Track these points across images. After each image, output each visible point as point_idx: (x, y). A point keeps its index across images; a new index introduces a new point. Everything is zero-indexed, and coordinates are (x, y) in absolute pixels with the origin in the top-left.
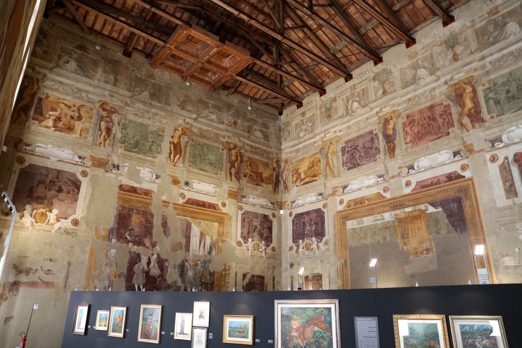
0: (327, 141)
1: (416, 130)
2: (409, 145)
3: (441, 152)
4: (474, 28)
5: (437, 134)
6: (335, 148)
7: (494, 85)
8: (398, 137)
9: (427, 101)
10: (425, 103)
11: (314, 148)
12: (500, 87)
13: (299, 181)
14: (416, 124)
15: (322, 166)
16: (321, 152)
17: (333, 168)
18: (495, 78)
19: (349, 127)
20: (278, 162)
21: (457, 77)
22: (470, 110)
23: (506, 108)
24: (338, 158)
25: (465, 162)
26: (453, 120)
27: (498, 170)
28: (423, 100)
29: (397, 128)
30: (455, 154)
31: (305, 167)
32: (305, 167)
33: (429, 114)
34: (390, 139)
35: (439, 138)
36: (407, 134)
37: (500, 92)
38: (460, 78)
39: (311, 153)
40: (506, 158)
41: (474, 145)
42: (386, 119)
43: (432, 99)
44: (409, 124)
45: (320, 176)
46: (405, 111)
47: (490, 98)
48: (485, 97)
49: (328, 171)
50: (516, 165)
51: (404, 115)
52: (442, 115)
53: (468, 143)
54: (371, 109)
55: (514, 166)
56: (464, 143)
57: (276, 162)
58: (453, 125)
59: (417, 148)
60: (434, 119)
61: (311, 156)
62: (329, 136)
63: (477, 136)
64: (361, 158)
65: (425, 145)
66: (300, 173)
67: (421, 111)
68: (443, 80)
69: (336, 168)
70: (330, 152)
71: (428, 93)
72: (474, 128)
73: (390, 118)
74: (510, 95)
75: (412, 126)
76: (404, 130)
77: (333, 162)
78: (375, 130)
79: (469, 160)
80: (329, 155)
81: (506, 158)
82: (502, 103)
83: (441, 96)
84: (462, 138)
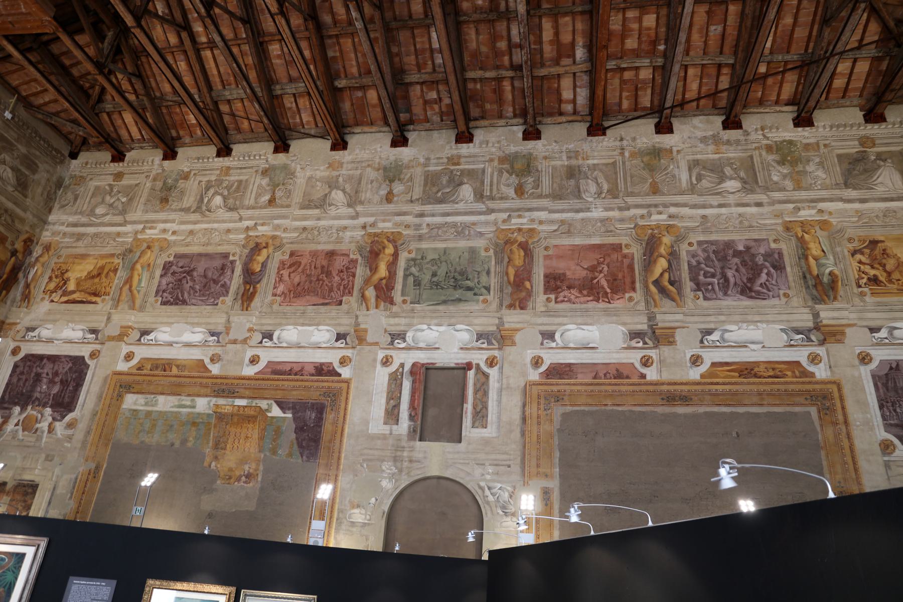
0: (144, 240)
1: (297, 280)
2: (278, 298)
3: (321, 327)
4: (427, 169)
5: (324, 298)
6: (152, 258)
7: (422, 258)
8: (265, 281)
9: (329, 243)
10: (325, 243)
11: (115, 244)
12: (428, 263)
13: (60, 292)
14: (300, 270)
15: (116, 281)
16: (124, 255)
17: (135, 292)
18: (427, 249)
19: (191, 232)
20: (29, 243)
21: (381, 225)
22: (381, 280)
23: (424, 297)
24: (152, 277)
25: (348, 353)
26: (353, 285)
27: (387, 378)
28: (323, 238)
29: (269, 264)
30: (340, 337)
31: (82, 271)
32: (82, 271)
33: (325, 263)
34: (251, 278)
35: (326, 304)
36: (281, 280)
37: (425, 271)
38: (384, 228)
39: (105, 251)
40: (402, 365)
41: (369, 332)
42: (257, 244)
43: (338, 243)
44: (290, 267)
45: (107, 297)
46: (291, 243)
47: (411, 274)
48: (406, 270)
49: (124, 294)
50: (411, 379)
51: (288, 248)
52: (342, 271)
53: (362, 326)
54: (241, 219)
55: (407, 379)
56: (357, 324)
57: (25, 241)
58: (350, 293)
59: (288, 308)
60: (329, 274)
61: (103, 257)
62: (151, 234)
63: (376, 321)
64: (192, 292)
65: (302, 308)
66: (68, 279)
67: (314, 254)
68: (362, 220)
69: (142, 293)
70: (141, 261)
71: (334, 231)
72: (377, 307)
73: (264, 245)
74: (435, 279)
75: (293, 272)
76: (278, 273)
77: (140, 281)
78: (233, 255)
79: (355, 352)
80: (138, 266)
81: (402, 365)
82: (422, 287)
83: (350, 242)
84: (357, 317)
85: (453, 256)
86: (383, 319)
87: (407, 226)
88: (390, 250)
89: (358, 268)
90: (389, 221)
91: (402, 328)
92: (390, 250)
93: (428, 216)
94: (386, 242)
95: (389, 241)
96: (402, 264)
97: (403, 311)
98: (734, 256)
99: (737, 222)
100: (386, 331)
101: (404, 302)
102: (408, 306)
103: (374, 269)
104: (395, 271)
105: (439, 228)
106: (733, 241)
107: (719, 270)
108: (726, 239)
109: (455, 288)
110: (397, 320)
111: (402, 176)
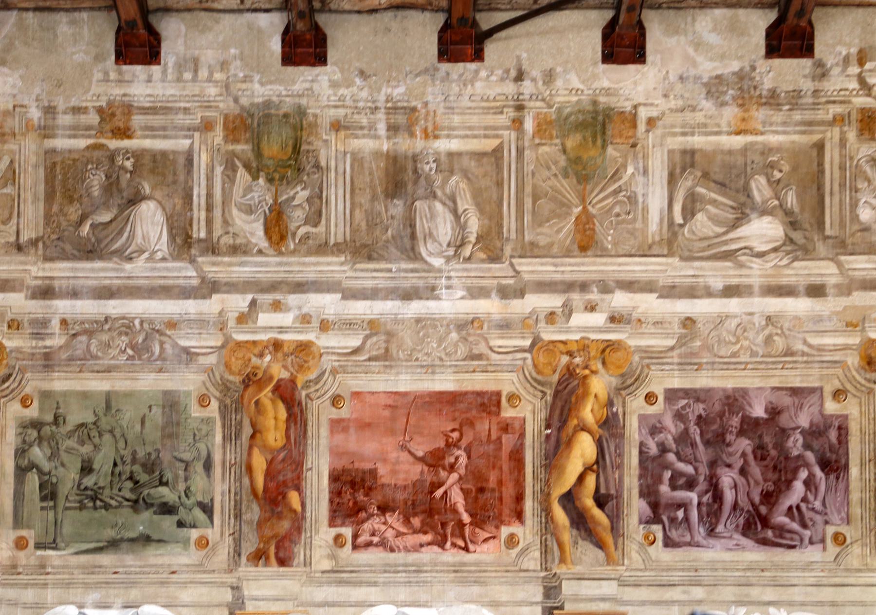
85: (128, 415)
98: (741, 433)
99: (760, 338)
106: (744, 392)
107: (704, 470)
108: (730, 384)
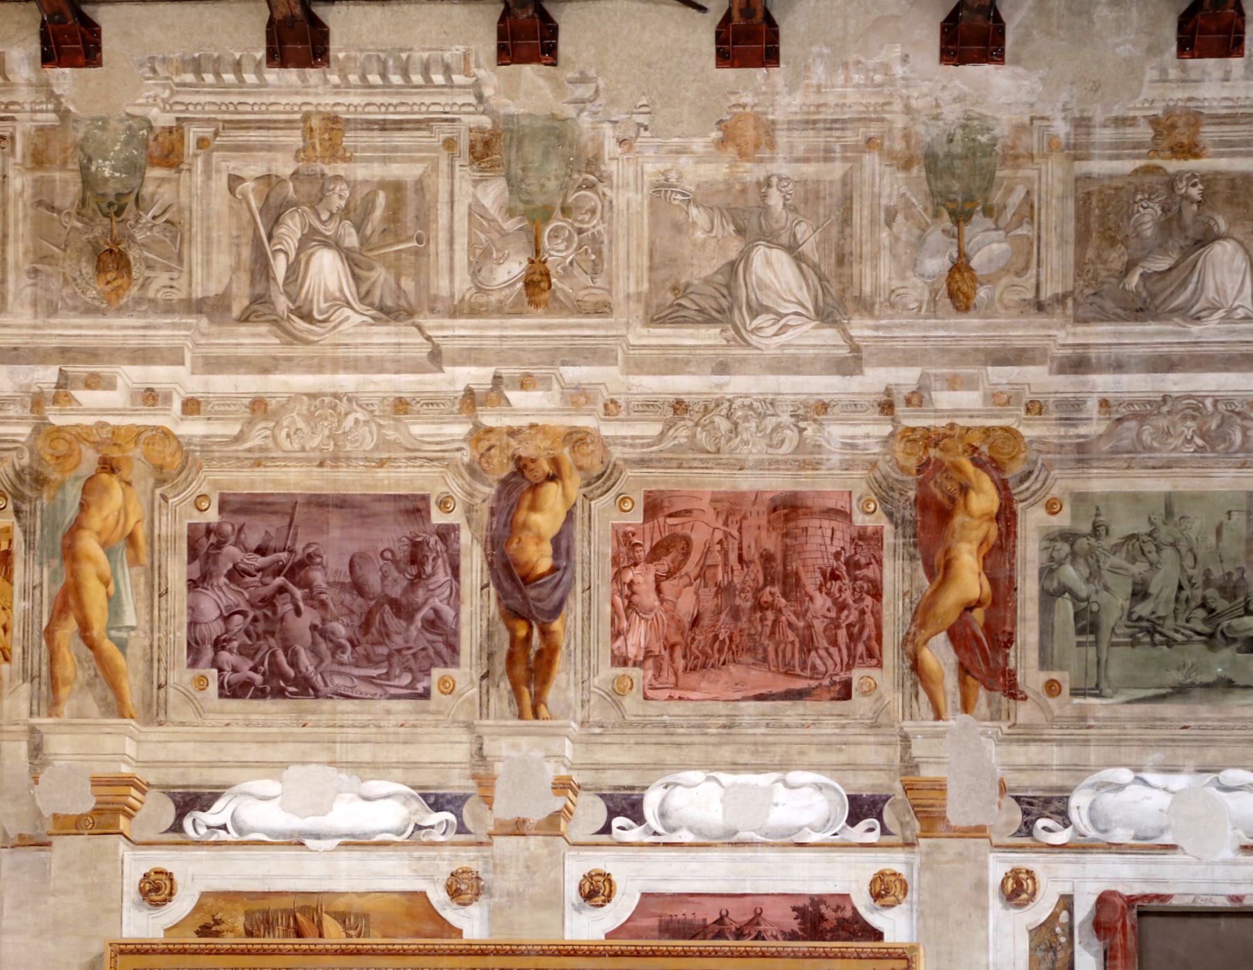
22: (969, 608)
23: (1114, 671)
48: (1047, 572)
72: (966, 707)
82: (1105, 636)
86: (991, 748)
87: (1035, 408)
88: (984, 499)
89: (887, 562)
90: (970, 384)
91: (1055, 779)
92: (984, 499)
93: (1100, 368)
94: (969, 468)
95: (977, 463)
96: (1029, 552)
97: (1053, 721)
100: (1003, 789)
101: (1052, 688)
102: (1065, 705)
103: (940, 570)
104: (1011, 579)
105: (1141, 418)
109: (1210, 640)
110: (1033, 753)
111: (996, 197)
